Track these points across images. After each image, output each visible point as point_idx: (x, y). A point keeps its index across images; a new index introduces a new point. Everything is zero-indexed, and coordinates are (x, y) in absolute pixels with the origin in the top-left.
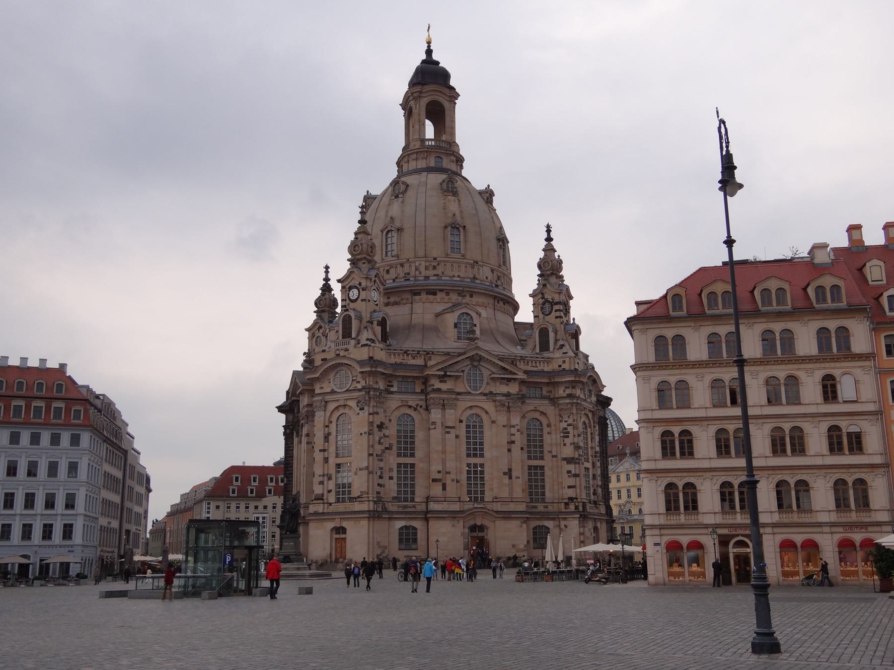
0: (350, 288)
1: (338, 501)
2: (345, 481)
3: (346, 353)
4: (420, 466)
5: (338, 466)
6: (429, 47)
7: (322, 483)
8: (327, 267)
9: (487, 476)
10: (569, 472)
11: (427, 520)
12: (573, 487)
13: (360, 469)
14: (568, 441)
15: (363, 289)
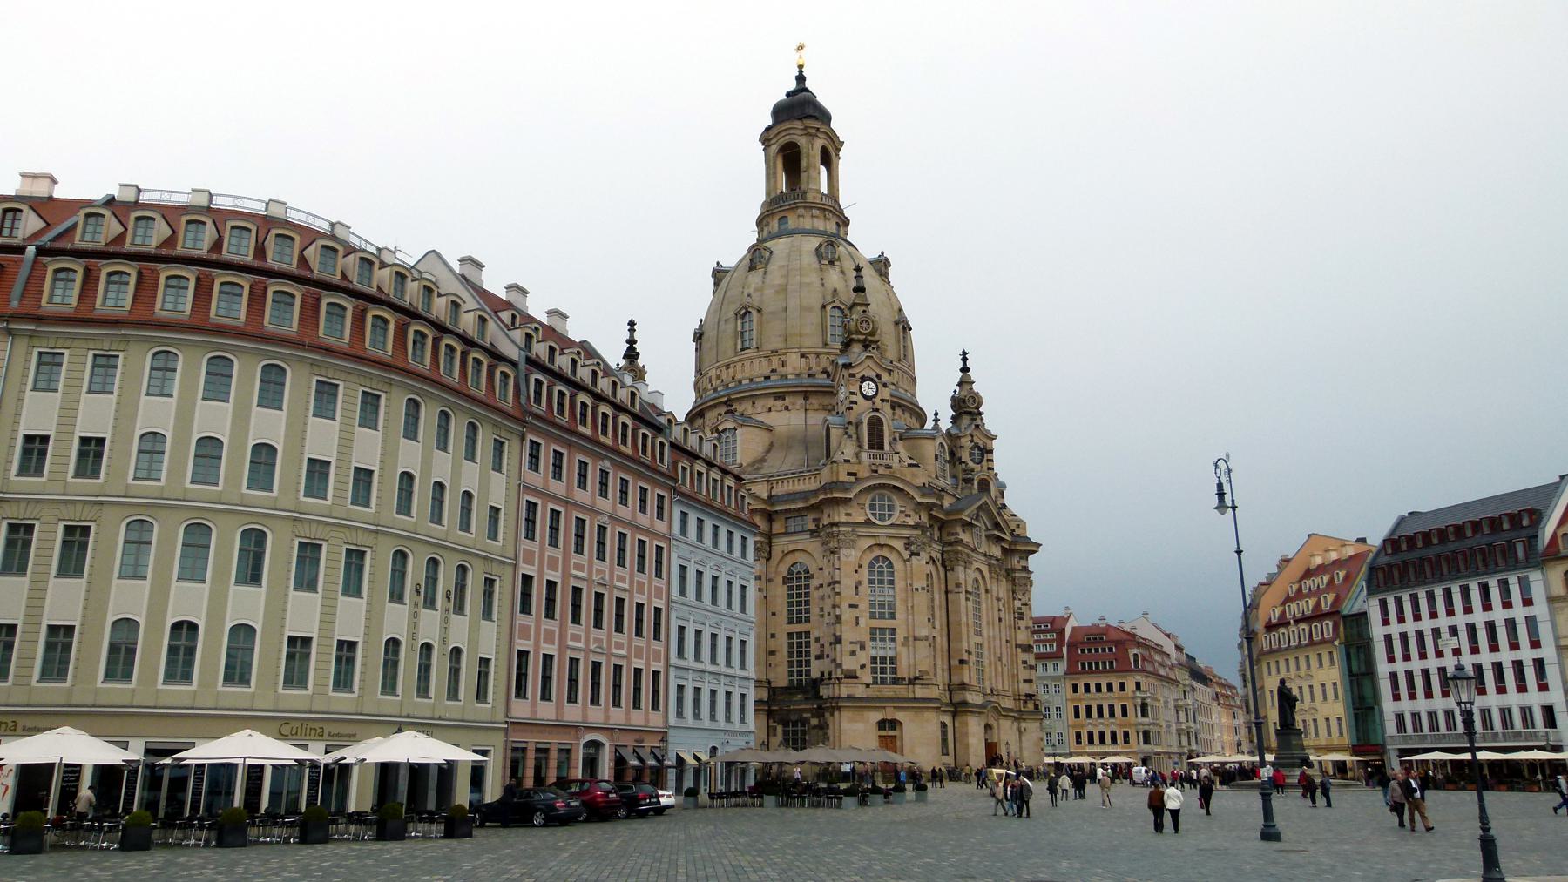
0: (863, 379)
1: (875, 683)
2: (881, 653)
3: (888, 472)
4: (938, 639)
5: (873, 630)
6: (801, 72)
7: (853, 653)
8: (632, 323)
9: (986, 662)
10: (1025, 662)
11: (954, 715)
12: (1030, 681)
13: (915, 639)
14: (1022, 624)
15: (885, 385)
